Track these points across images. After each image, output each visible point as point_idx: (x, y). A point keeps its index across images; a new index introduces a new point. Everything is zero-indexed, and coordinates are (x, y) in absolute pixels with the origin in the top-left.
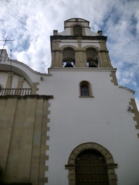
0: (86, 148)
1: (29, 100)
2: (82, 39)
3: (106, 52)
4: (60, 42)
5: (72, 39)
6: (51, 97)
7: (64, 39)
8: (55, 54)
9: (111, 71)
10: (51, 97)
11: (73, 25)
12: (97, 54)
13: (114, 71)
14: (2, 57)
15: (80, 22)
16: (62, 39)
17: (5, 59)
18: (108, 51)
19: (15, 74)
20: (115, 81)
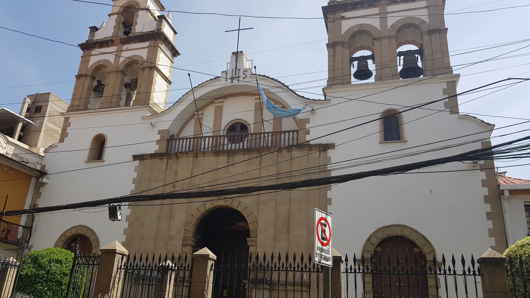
0: (390, 235)
1: (296, 153)
4: (343, 18)
5: (367, 8)
6: (331, 146)
7: (351, 10)
8: (335, 51)
9: (446, 82)
10: (331, 146)
14: (239, 70)
16: (346, 11)
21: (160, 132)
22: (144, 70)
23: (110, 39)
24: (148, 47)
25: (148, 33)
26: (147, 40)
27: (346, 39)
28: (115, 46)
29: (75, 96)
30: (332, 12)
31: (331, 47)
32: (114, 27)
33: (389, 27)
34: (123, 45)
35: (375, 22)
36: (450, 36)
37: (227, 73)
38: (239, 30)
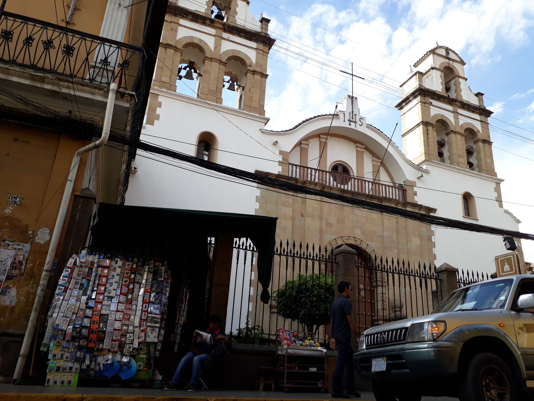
2: (459, 108)
3: (489, 144)
5: (446, 103)
7: (436, 99)
8: (427, 130)
9: (496, 183)
11: (442, 63)
12: (475, 143)
13: (498, 182)
14: (355, 115)
15: (454, 60)
16: (433, 98)
17: (360, 121)
18: (493, 143)
19: (367, 148)
20: (499, 200)
21: (281, 153)
22: (254, 74)
23: (204, 15)
24: (256, 49)
25: (252, 31)
26: (256, 41)
27: (434, 123)
28: (212, 28)
29: (163, 69)
30: (423, 94)
31: (425, 125)
32: (207, 3)
33: (460, 125)
34: (223, 32)
35: (450, 117)
36: (495, 149)
37: (344, 114)
38: (352, 75)
